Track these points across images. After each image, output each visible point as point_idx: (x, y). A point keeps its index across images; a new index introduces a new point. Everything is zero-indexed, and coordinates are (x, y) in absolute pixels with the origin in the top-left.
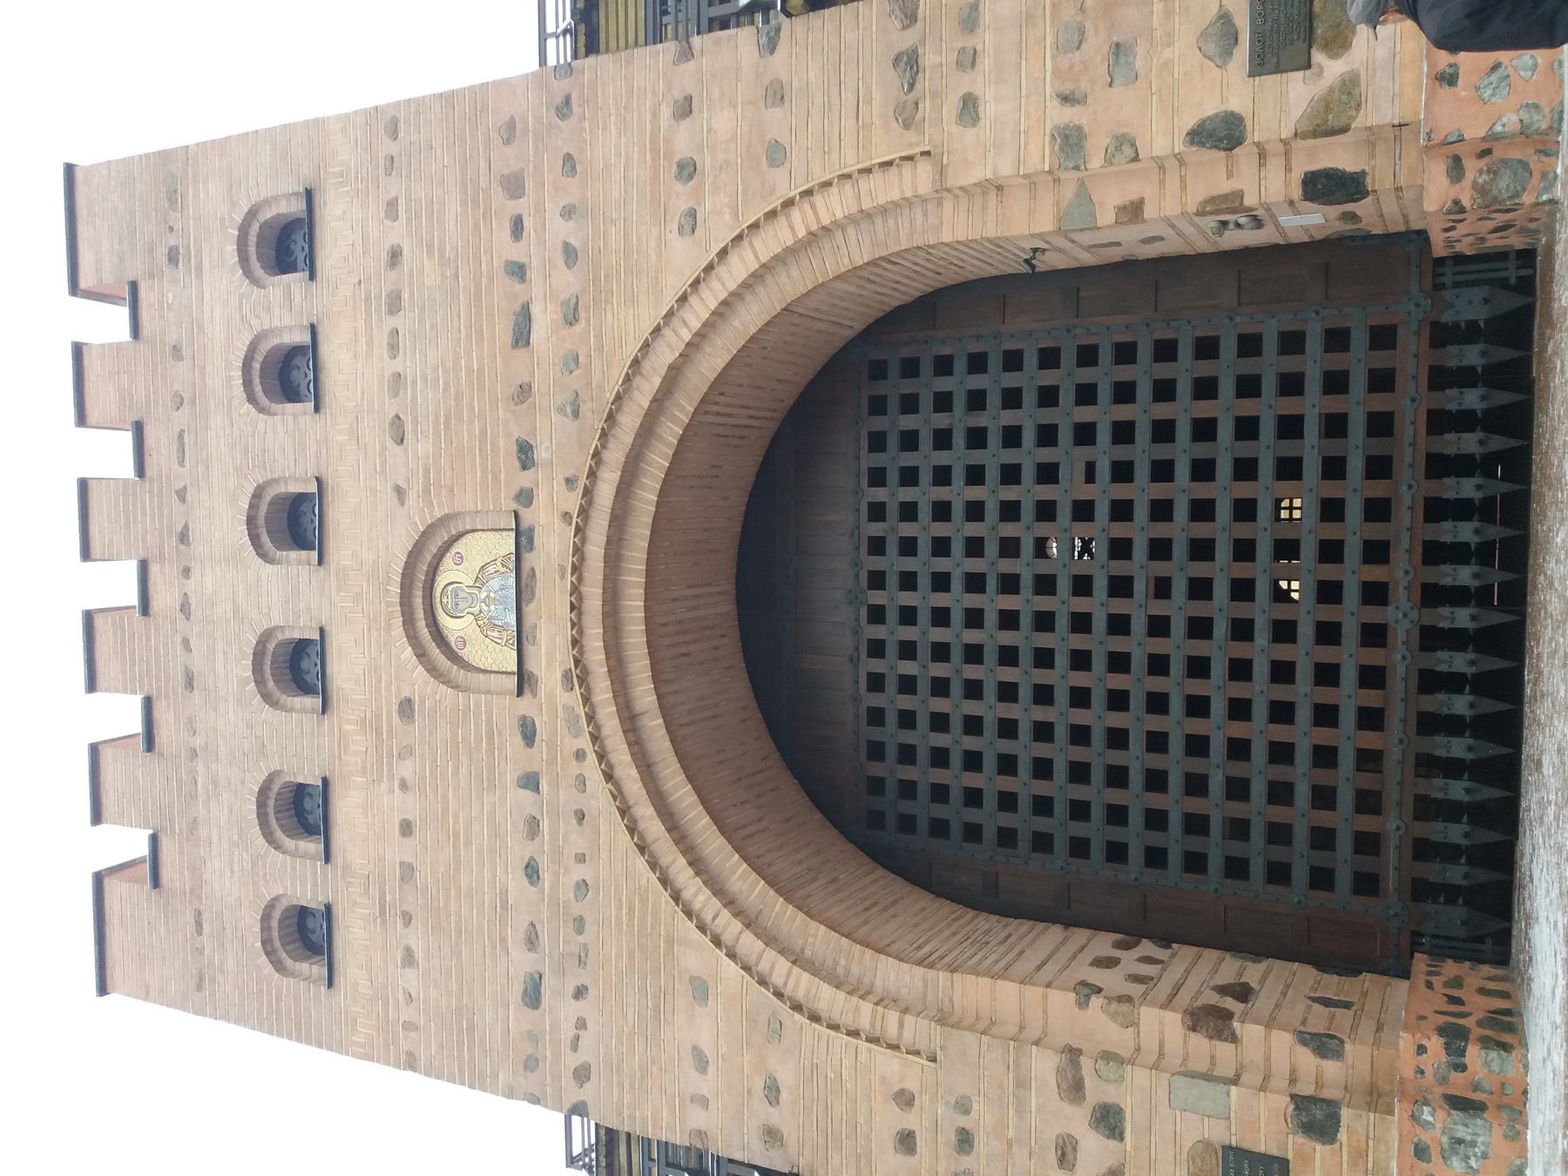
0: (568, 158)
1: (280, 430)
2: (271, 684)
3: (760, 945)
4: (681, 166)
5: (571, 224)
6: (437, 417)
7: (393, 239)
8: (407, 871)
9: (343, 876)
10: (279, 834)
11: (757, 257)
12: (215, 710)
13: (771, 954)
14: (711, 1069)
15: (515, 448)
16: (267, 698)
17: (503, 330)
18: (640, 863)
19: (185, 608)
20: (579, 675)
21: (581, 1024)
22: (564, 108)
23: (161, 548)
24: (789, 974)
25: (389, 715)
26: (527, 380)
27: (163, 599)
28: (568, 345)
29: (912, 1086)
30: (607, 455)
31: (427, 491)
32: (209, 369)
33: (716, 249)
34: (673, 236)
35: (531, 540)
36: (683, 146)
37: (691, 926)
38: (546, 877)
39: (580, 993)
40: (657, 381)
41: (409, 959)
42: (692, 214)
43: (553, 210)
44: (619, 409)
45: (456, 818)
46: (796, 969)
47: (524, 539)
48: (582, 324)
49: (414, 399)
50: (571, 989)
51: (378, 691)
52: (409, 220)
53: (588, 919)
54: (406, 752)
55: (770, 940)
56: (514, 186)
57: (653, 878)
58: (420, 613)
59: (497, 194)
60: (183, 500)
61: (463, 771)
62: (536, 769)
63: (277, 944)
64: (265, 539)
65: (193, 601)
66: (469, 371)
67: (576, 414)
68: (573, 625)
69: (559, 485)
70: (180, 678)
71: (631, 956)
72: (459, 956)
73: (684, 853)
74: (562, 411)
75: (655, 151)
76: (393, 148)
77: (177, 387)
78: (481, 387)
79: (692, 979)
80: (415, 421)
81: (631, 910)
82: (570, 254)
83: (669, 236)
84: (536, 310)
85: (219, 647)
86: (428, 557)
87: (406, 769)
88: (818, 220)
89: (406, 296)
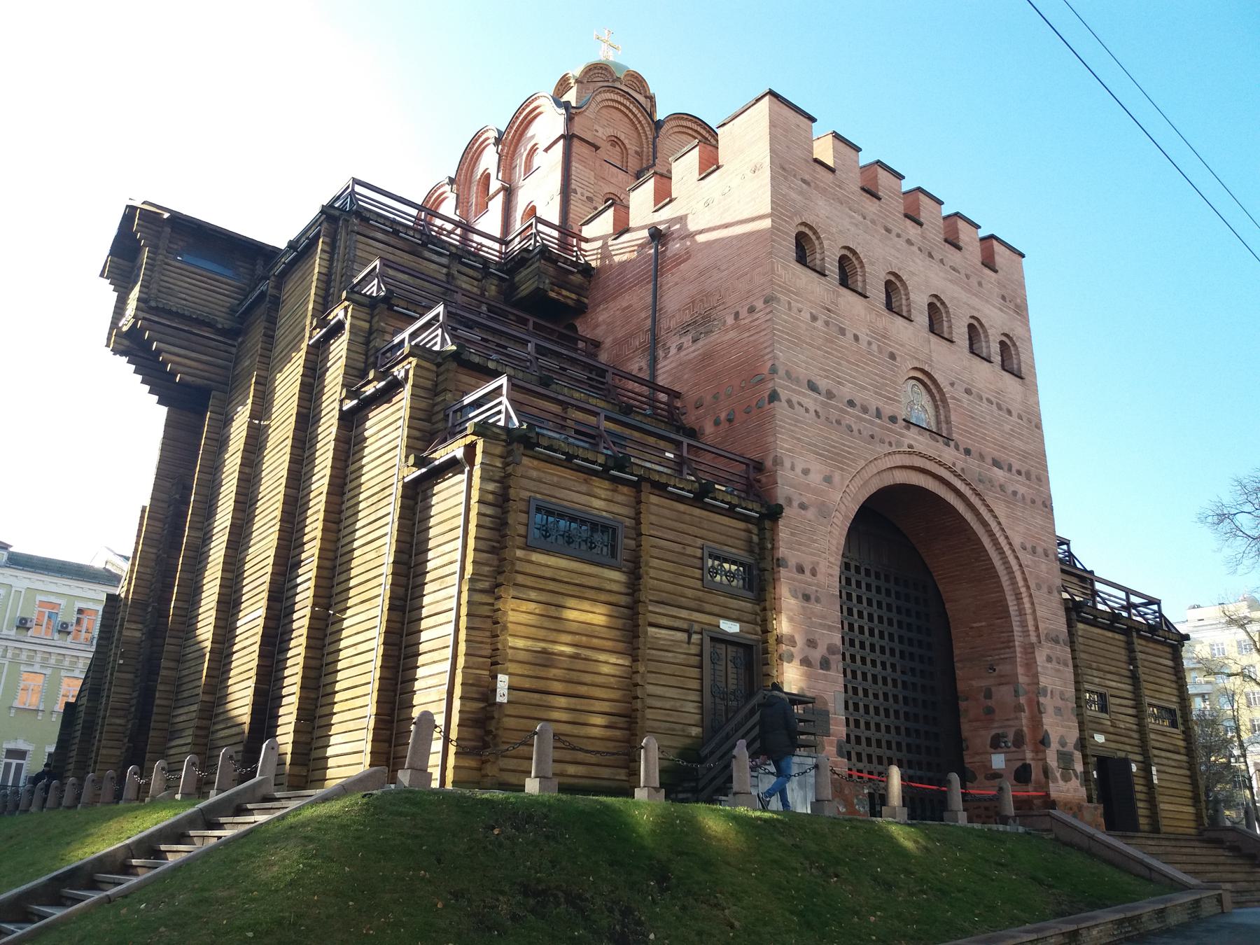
8: (842, 332)
17: (996, 454)
18: (863, 463)
19: (909, 242)
20: (911, 453)
29: (819, 576)
47: (948, 440)
56: (1028, 478)
58: (929, 383)
81: (849, 453)
87: (874, 347)
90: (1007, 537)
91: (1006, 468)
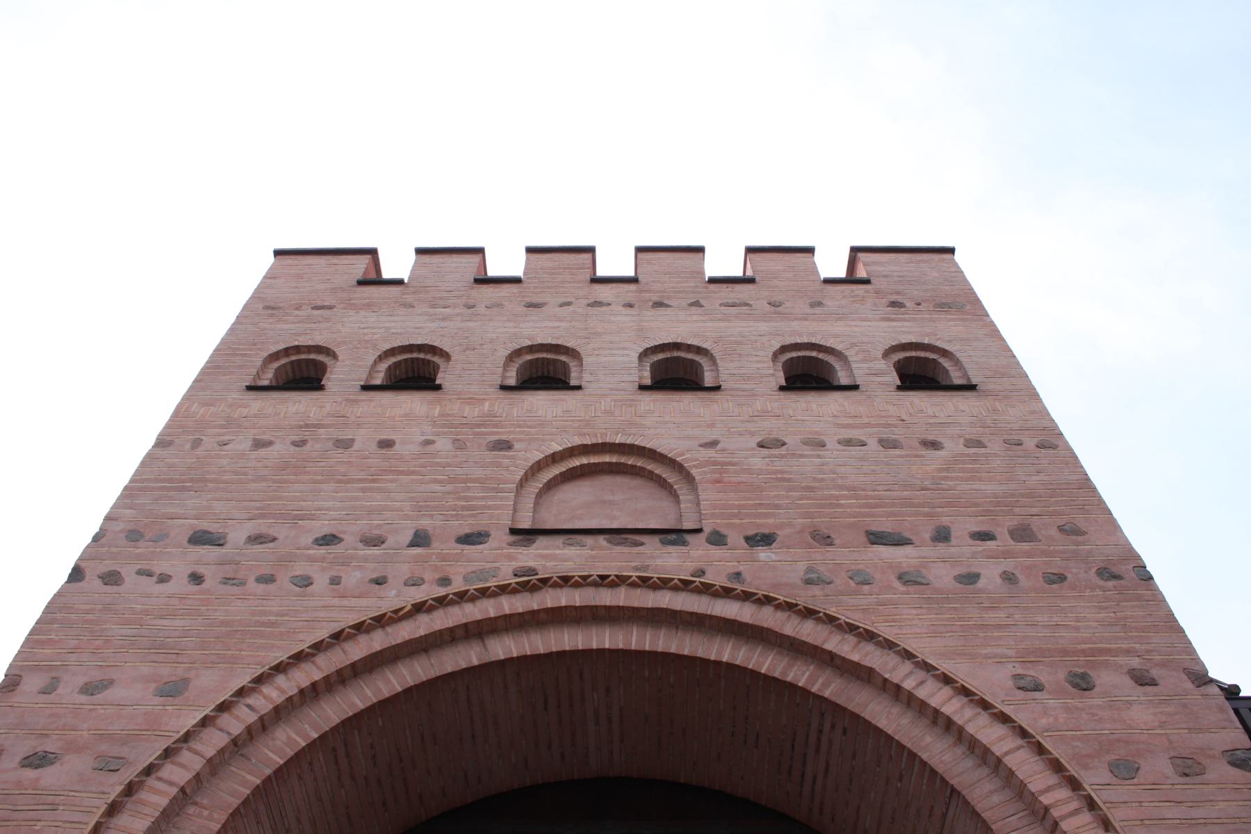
0: (1061, 578)
1: (760, 365)
2: (529, 357)
3: (210, 752)
4: (1084, 676)
5: (999, 581)
6: (791, 473)
7: (947, 443)
8: (345, 444)
9: (348, 400)
10: (393, 360)
11: (1007, 754)
12: (509, 321)
13: (197, 764)
14: (84, 698)
15: (766, 531)
16: (518, 353)
18: (322, 633)
20: (530, 583)
21: (164, 579)
22: (1107, 573)
23: (649, 291)
24: (171, 784)
25: (497, 433)
26: (837, 542)
27: (603, 292)
28: (878, 576)
30: (768, 611)
31: (715, 463)
32: (807, 323)
33: (1008, 710)
34: (1010, 669)
35: (673, 543)
36: (1105, 679)
37: (244, 680)
38: (322, 551)
39: (196, 578)
40: (855, 657)
41: (259, 444)
42: (1038, 688)
43: (1008, 565)
44: (819, 620)
45: (391, 481)
46: (174, 791)
47: (673, 535)
48: (903, 588)
49: (802, 456)
50: (201, 570)
51: (520, 426)
52: (968, 455)
53: (271, 587)
54: (459, 445)
55: (215, 766)
56: (1022, 533)
57: (304, 646)
59: (1011, 522)
60: (691, 305)
61: (437, 487)
62: (434, 545)
63: (294, 358)
64: (660, 356)
65: (604, 308)
66: (837, 498)
67: (809, 582)
68: (584, 578)
69: (733, 567)
70: (535, 300)
71: (224, 623)
72: (253, 481)
73: (327, 679)
74: (810, 570)
75: (1093, 652)
76: (1030, 443)
77: (787, 304)
78: (823, 506)
79: (186, 681)
80: (783, 456)
81: (272, 624)
82: (970, 578)
83: (1010, 666)
84: (908, 550)
85: (563, 324)
86: (651, 466)
87: (443, 444)
88: (1063, 818)
89: (897, 452)
90: (947, 680)
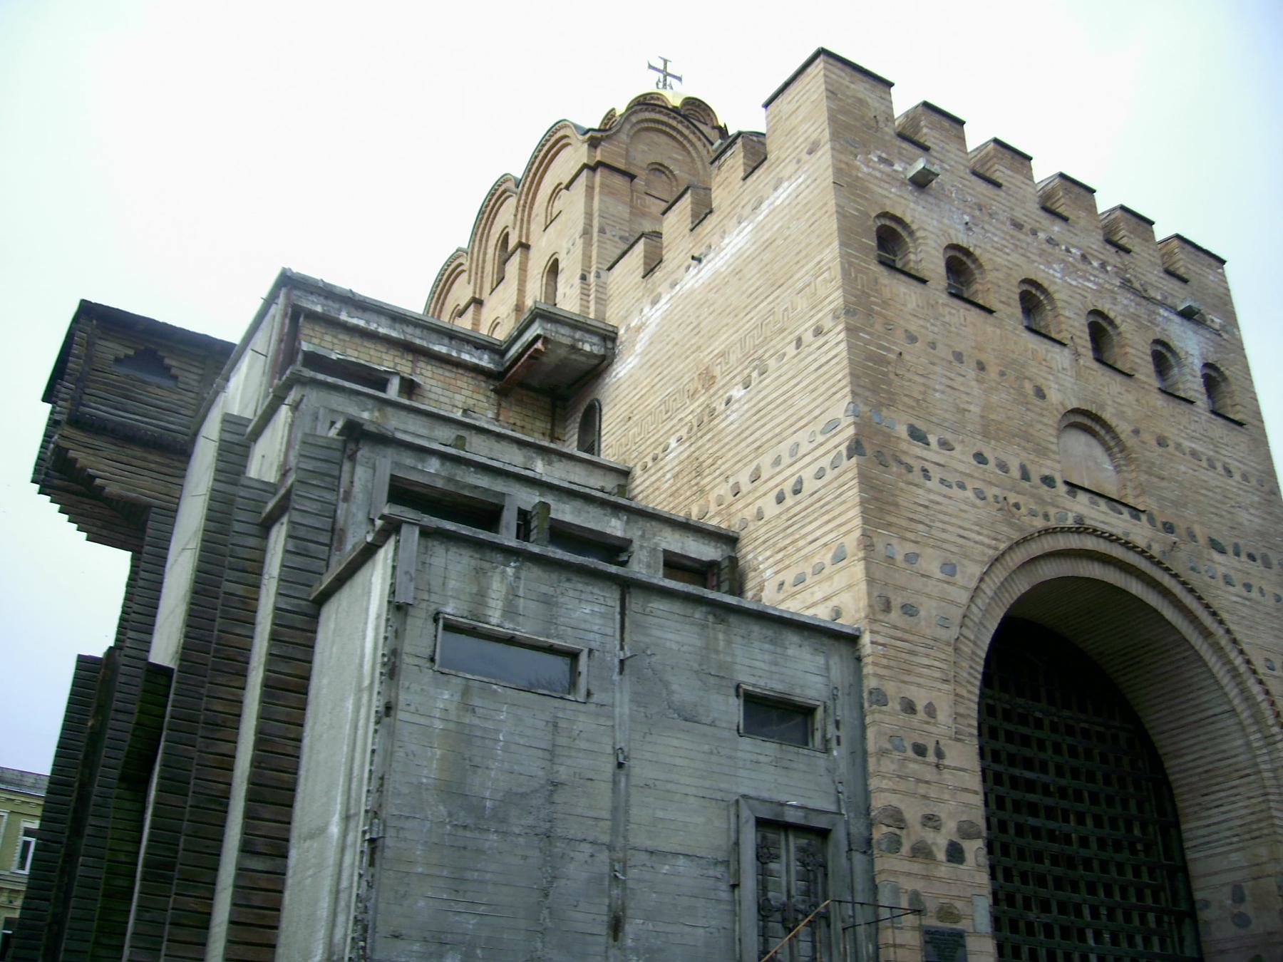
20: (1081, 529)
67: (1193, 569)
91: (1230, 550)
